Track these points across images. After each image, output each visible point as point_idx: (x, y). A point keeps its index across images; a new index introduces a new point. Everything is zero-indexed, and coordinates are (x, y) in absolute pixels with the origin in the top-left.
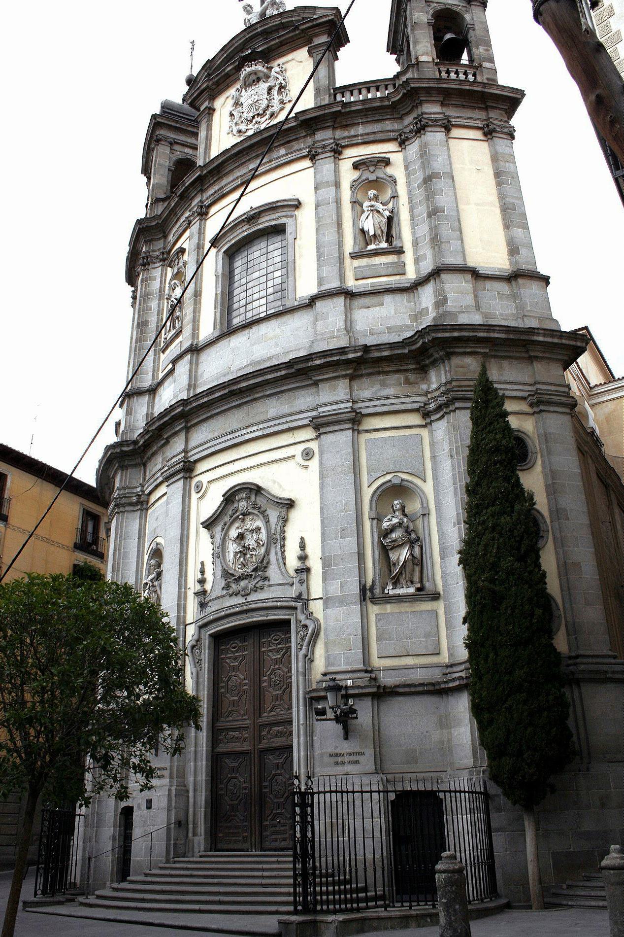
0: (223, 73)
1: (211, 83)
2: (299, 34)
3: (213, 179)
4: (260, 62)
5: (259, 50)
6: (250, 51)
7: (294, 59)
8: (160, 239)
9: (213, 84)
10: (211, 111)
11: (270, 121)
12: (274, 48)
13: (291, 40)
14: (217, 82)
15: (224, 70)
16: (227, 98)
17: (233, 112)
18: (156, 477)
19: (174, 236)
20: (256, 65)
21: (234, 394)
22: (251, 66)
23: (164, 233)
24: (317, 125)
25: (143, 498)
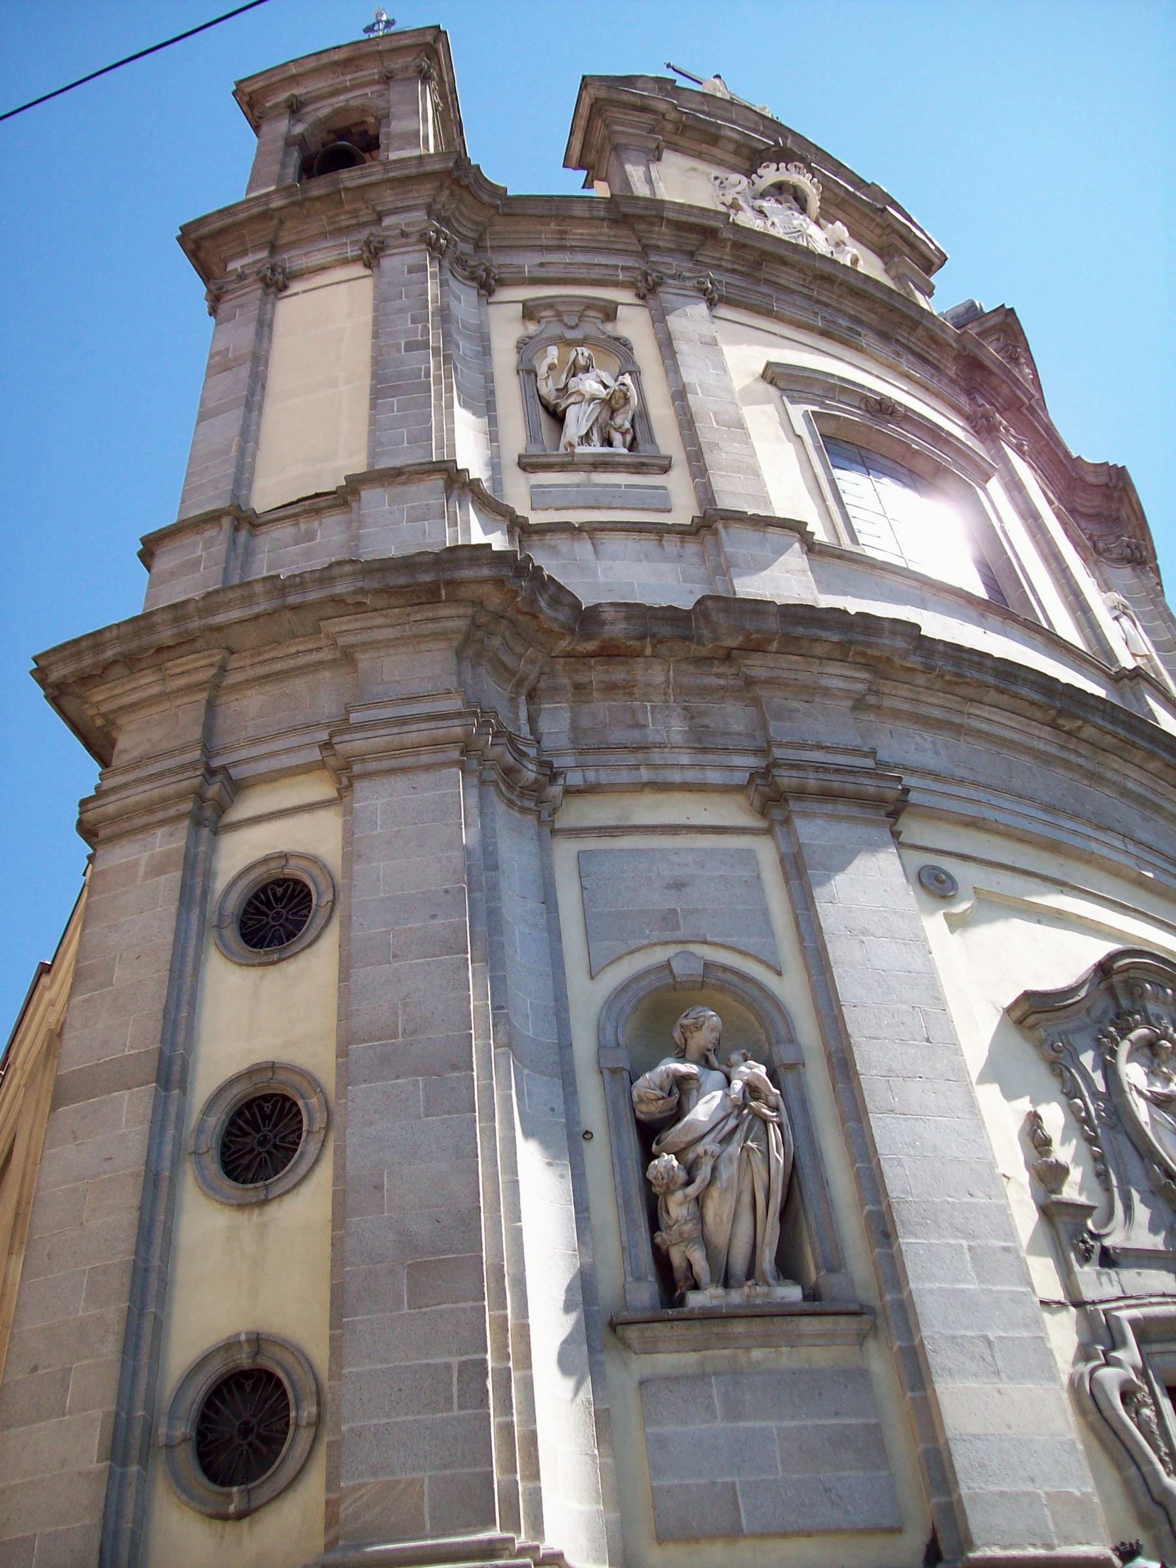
3: (733, 262)
4: (818, 189)
8: (464, 239)
16: (694, 169)
18: (657, 757)
19: (542, 265)
21: (1054, 726)
23: (481, 237)
24: (982, 386)
25: (555, 790)
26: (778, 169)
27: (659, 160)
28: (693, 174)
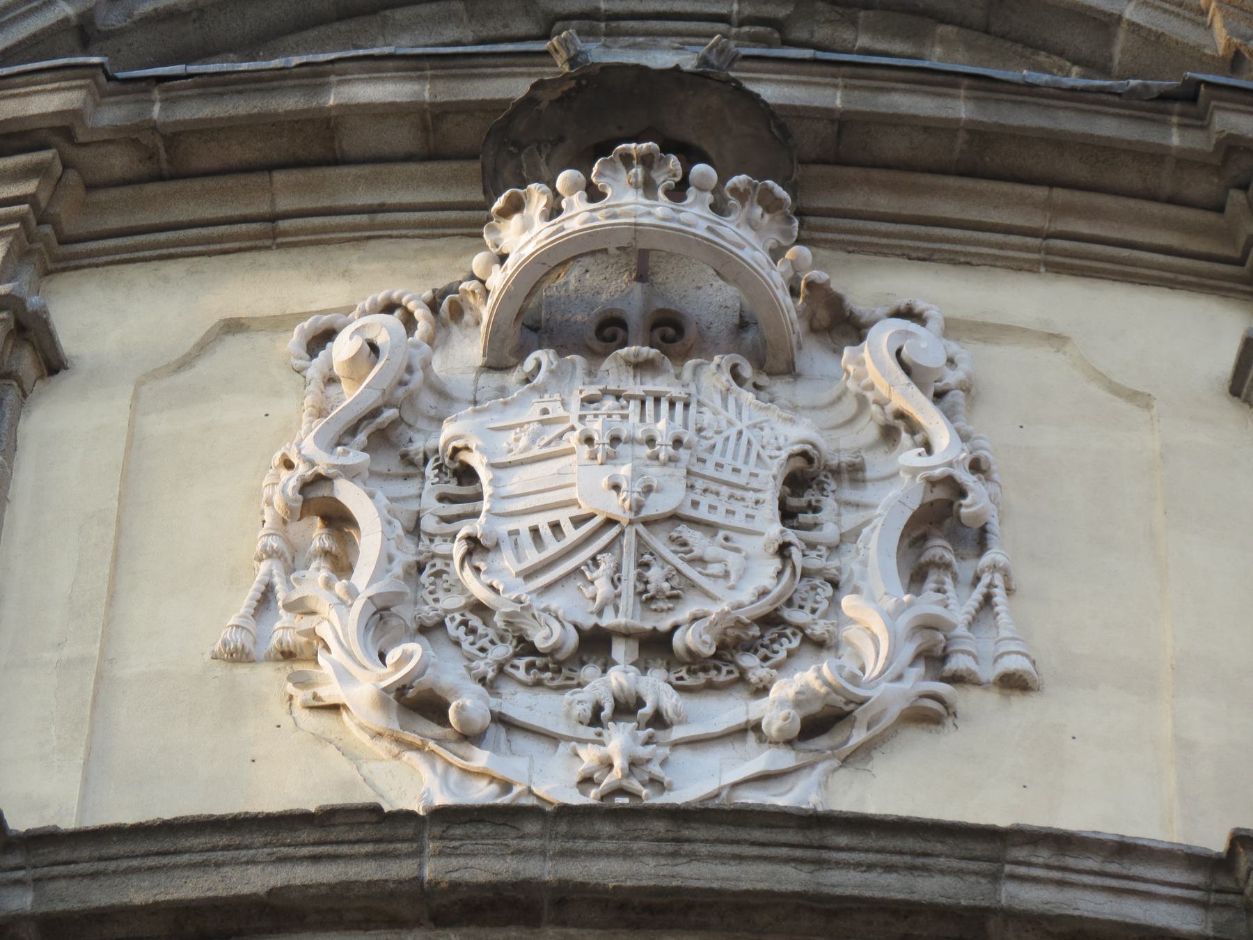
0: (289, 102)
1: (112, 115)
2: (1185, 162)
4: (770, 204)
5: (772, 92)
6: (688, 61)
7: (1056, 339)
9: (130, 137)
10: (26, 363)
11: (785, 759)
12: (894, 145)
13: (1075, 168)
14: (175, 137)
15: (316, 76)
17: (349, 494)
20: (719, 208)
22: (678, 192)
26: (554, 211)
27: (53, 364)
28: (235, 344)
